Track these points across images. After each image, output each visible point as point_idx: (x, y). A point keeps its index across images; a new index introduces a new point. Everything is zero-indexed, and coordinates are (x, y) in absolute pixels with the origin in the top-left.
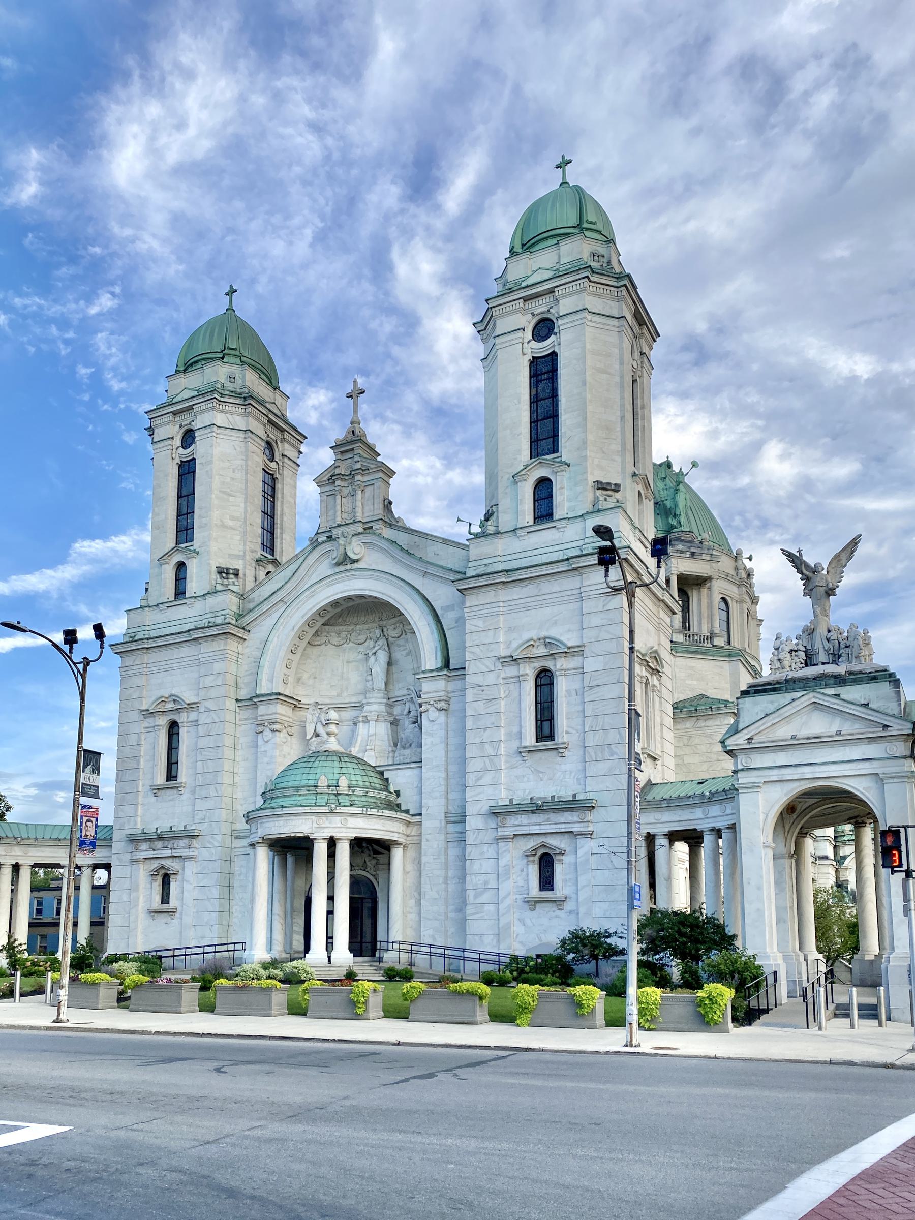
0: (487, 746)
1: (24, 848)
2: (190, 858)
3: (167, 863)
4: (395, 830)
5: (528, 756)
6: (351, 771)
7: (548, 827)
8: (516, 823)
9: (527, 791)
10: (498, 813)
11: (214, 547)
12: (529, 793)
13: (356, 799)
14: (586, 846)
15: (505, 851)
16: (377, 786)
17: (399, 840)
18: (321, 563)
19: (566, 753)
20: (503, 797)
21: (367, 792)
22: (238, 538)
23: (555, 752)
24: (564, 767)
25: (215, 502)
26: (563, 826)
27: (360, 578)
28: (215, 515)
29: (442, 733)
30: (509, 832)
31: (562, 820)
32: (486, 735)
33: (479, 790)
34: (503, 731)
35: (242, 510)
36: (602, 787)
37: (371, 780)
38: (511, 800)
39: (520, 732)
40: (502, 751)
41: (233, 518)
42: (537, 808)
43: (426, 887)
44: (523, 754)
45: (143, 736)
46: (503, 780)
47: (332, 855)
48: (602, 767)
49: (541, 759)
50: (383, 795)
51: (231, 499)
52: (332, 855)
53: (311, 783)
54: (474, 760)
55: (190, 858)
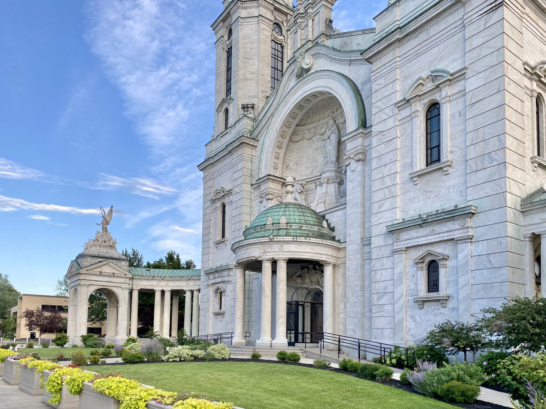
0: (386, 179)
1: (166, 282)
2: (229, 282)
3: (220, 285)
4: (324, 253)
5: (418, 181)
6: (292, 213)
7: (433, 237)
8: (408, 237)
9: (418, 210)
10: (394, 231)
11: (240, 93)
12: (419, 211)
13: (293, 231)
14: (467, 249)
15: (399, 261)
16: (311, 222)
17: (328, 260)
18: (291, 81)
19: (450, 170)
20: (399, 216)
21: (301, 227)
22: (254, 84)
23: (441, 172)
24: (447, 184)
25: (241, 65)
26: (446, 234)
27: (310, 82)
28: (241, 73)
29: (359, 178)
30: (402, 245)
31: (445, 229)
32: (386, 171)
33: (381, 215)
34: (398, 164)
35: (257, 67)
36: (482, 194)
37: (306, 218)
38: (404, 219)
39: (412, 162)
40: (398, 181)
41: (251, 73)
42: (423, 222)
43: (349, 294)
44: (414, 179)
45: (212, 216)
46: (398, 204)
47: (274, 272)
48: (482, 176)
49: (429, 180)
50: (316, 228)
51: (250, 61)
52: (274, 272)
53: (263, 223)
54: (377, 193)
55: (229, 282)
